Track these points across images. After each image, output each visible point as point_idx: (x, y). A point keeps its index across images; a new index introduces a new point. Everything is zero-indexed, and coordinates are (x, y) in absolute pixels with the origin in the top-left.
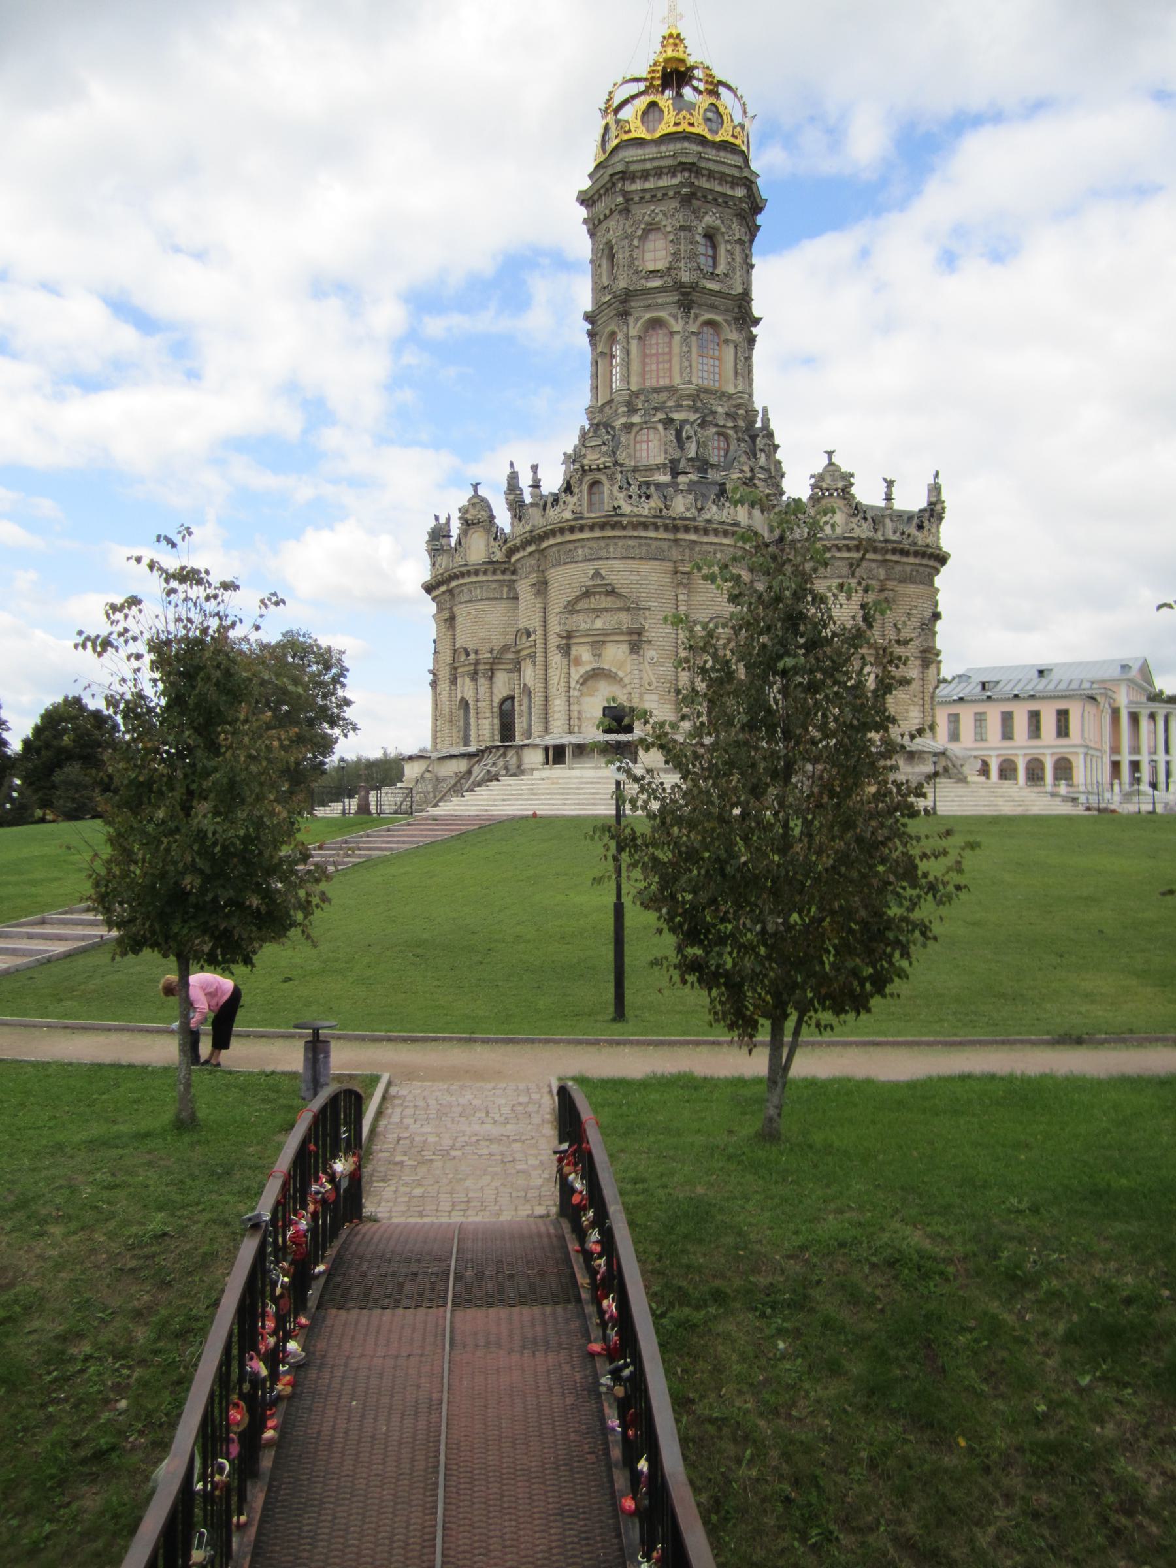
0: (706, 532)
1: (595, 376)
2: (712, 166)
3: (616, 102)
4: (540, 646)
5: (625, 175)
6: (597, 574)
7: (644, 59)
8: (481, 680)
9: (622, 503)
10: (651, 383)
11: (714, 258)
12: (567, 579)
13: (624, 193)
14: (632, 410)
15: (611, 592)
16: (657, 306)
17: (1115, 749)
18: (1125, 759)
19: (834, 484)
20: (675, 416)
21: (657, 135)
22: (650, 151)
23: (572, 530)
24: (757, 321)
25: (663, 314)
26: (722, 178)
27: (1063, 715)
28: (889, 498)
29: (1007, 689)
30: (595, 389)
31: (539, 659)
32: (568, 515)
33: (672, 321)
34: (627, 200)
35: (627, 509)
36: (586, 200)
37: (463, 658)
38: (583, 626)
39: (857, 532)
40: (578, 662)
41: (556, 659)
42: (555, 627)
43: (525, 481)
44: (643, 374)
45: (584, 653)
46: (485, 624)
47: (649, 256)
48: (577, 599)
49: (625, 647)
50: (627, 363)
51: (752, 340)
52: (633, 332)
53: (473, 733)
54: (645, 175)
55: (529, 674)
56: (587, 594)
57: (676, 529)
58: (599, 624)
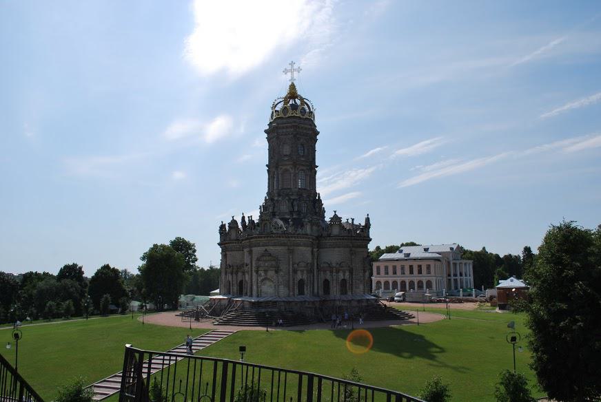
1: (269, 183)
3: (276, 103)
5: (277, 128)
6: (266, 250)
7: (284, 93)
8: (234, 275)
10: (285, 187)
11: (304, 150)
12: (257, 251)
14: (279, 195)
15: (270, 255)
16: (286, 165)
17: (449, 275)
18: (453, 278)
19: (336, 218)
25: (288, 167)
27: (428, 267)
28: (353, 222)
29: (411, 256)
30: (269, 187)
31: (250, 273)
32: (258, 233)
35: (274, 232)
36: (266, 131)
40: (260, 275)
41: (254, 274)
42: (254, 265)
46: (235, 257)
47: (285, 150)
49: (274, 272)
50: (278, 181)
51: (315, 172)
54: (283, 128)
57: (289, 237)
58: (266, 264)
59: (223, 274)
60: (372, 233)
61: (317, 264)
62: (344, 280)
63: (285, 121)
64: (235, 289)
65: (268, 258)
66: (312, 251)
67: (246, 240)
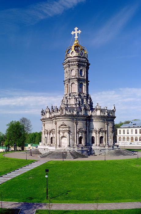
0: (79, 117)
2: (81, 61)
4: (56, 132)
6: (63, 122)
9: (67, 113)
12: (59, 123)
13: (69, 65)
15: (65, 125)
16: (73, 81)
20: (76, 97)
21: (73, 56)
22: (72, 58)
23: (60, 116)
24: (89, 81)
26: (83, 62)
31: (56, 134)
32: (59, 114)
33: (76, 83)
34: (69, 65)
37: (46, 131)
38: (61, 130)
39: (102, 115)
41: (58, 134)
42: (58, 130)
43: (54, 108)
44: (71, 91)
45: (61, 133)
48: (60, 126)
52: (70, 84)
53: (47, 142)
55: (54, 135)
56: (62, 125)
57: (74, 116)
58: (63, 130)
59: (43, 134)
60: (116, 114)
61: (89, 130)
62: (102, 137)
63: (72, 58)
64: (49, 141)
65: (65, 127)
66: (86, 123)
67: (53, 118)
